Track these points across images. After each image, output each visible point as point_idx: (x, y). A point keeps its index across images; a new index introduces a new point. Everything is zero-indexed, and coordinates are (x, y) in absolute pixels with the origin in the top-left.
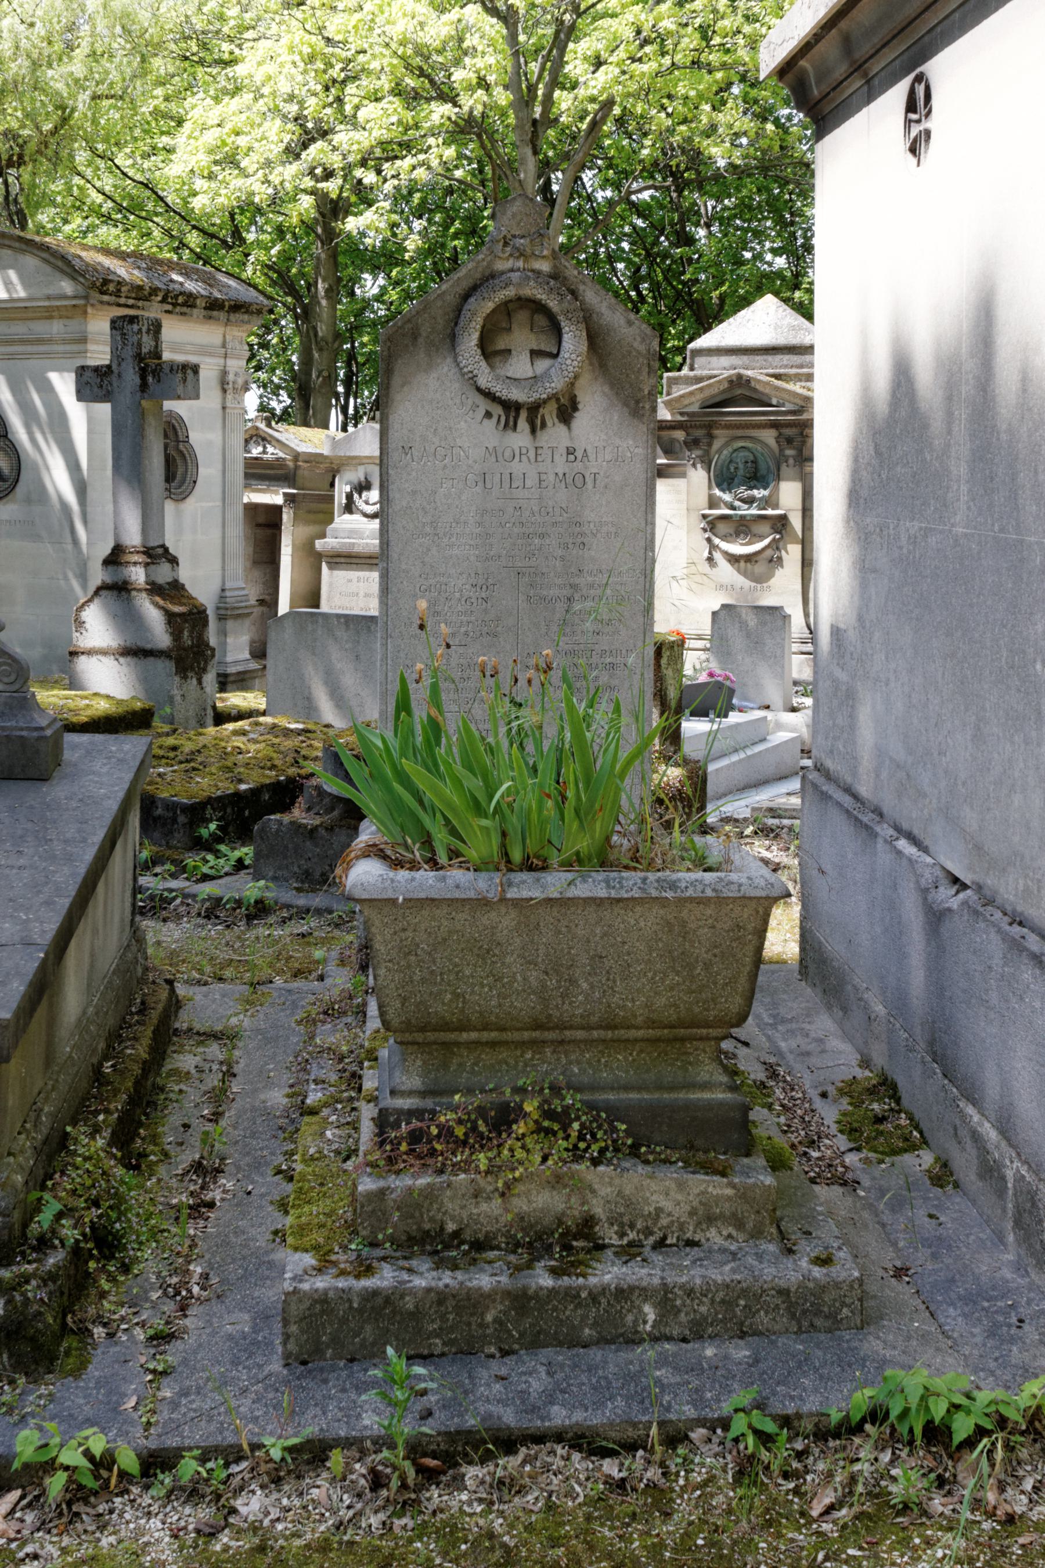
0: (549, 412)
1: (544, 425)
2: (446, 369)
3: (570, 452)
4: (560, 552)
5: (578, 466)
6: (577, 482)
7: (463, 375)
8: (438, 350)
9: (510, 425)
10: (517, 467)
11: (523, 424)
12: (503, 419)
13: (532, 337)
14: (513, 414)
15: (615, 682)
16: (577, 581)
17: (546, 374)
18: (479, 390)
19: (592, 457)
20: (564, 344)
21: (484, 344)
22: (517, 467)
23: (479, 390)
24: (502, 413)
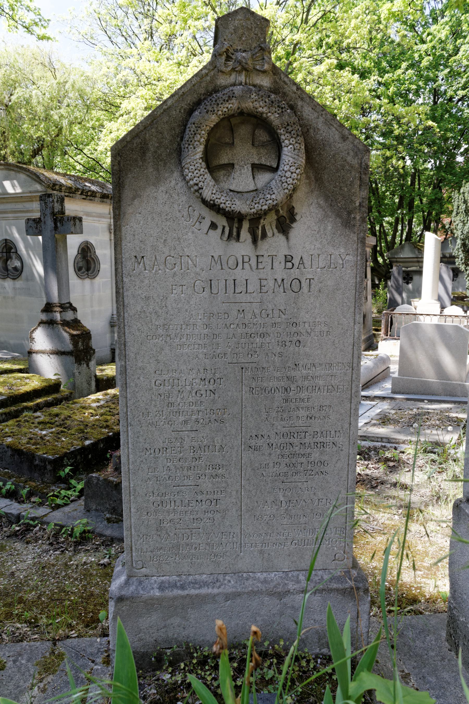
0: (269, 223)
1: (264, 235)
2: (173, 182)
3: (288, 259)
4: (278, 349)
5: (295, 273)
6: (295, 287)
8: (165, 164)
9: (234, 236)
10: (240, 274)
11: (245, 234)
14: (236, 225)
15: (325, 458)
16: (293, 373)
17: (267, 186)
18: (204, 201)
19: (307, 263)
22: (240, 274)
23: (204, 201)
24: (226, 224)
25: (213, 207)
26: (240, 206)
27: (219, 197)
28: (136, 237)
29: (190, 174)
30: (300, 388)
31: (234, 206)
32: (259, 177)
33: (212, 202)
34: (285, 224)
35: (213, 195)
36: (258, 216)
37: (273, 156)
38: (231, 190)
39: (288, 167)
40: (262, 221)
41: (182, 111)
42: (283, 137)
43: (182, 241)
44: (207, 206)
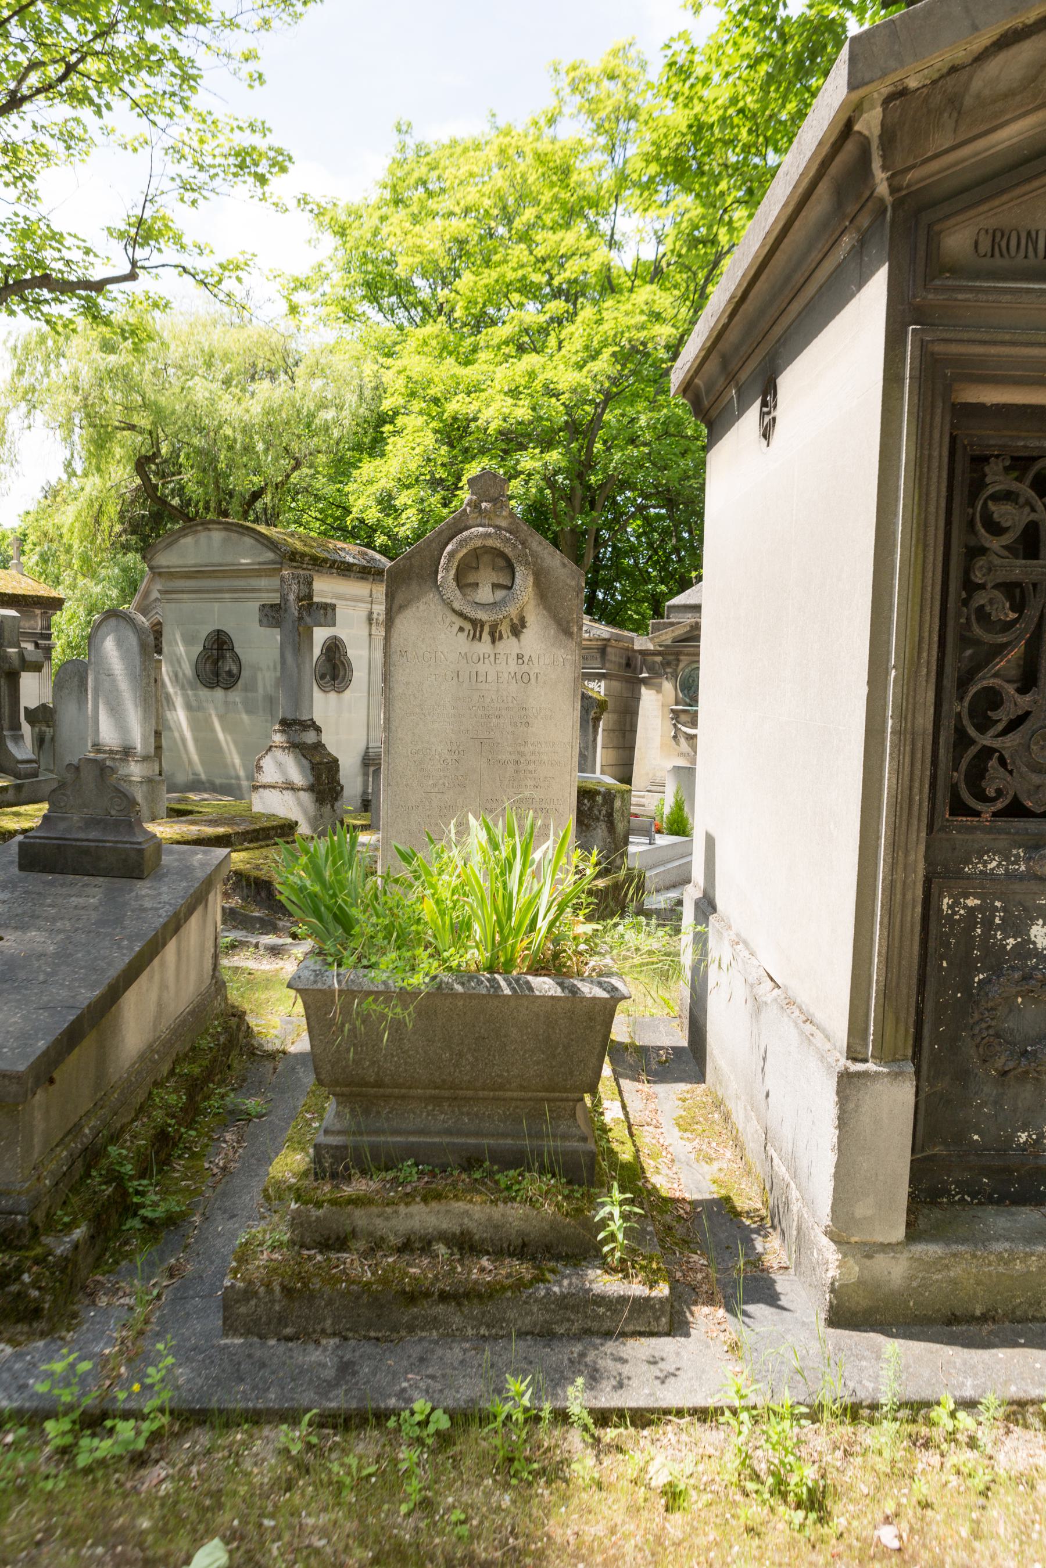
1: (501, 638)
3: (520, 657)
5: (525, 668)
6: (525, 679)
9: (476, 637)
10: (482, 668)
11: (486, 636)
13: (494, 574)
16: (522, 749)
18: (454, 611)
19: (535, 661)
21: (457, 578)
22: (482, 668)
23: (454, 611)
25: (461, 615)
26: (481, 615)
30: (529, 762)
34: (517, 629)
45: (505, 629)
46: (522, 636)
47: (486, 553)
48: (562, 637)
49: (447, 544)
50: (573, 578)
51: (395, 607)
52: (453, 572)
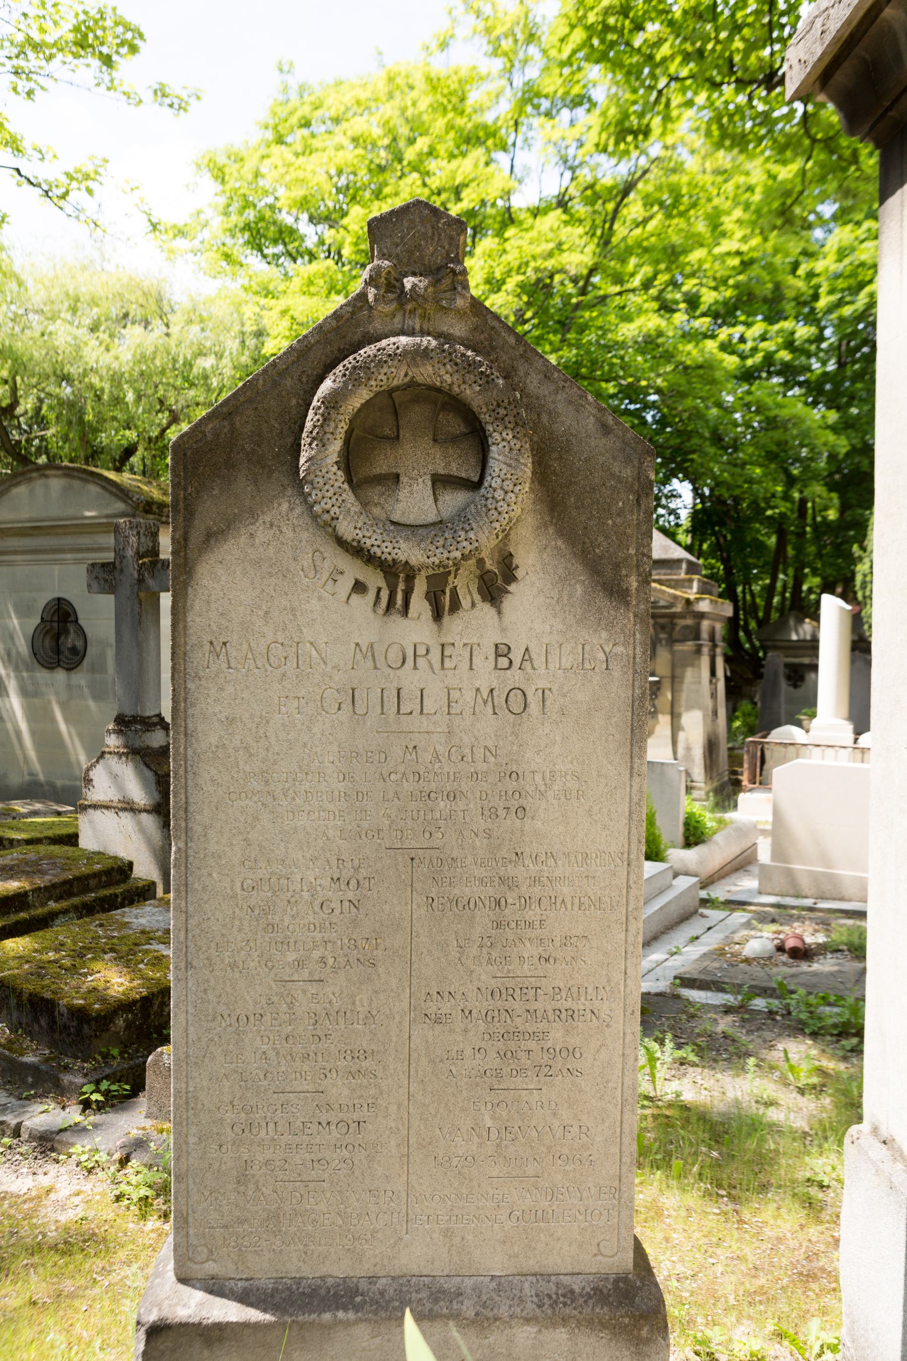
0: (464, 584)
1: (455, 606)
2: (285, 506)
3: (501, 651)
4: (481, 824)
5: (514, 677)
6: (515, 704)
7: (315, 517)
9: (396, 606)
10: (410, 680)
12: (385, 595)
13: (437, 453)
14: (401, 586)
16: (511, 870)
18: (341, 542)
19: (539, 661)
20: (491, 463)
22: (410, 680)
23: (341, 542)
24: (383, 584)
25: (357, 551)
26: (408, 552)
27: (368, 534)
28: (213, 605)
29: (314, 492)
30: (527, 902)
31: (396, 551)
32: (447, 498)
33: (355, 544)
34: (495, 586)
35: (358, 531)
36: (442, 570)
37: (473, 461)
38: (393, 523)
39: (499, 480)
40: (451, 578)
41: (304, 379)
42: (490, 428)
43: (298, 614)
44: (347, 551)
45: (464, 584)
46: (508, 603)
47: (416, 400)
48: (602, 601)
49: (321, 379)
50: (628, 460)
51: (196, 537)
52: (336, 447)
